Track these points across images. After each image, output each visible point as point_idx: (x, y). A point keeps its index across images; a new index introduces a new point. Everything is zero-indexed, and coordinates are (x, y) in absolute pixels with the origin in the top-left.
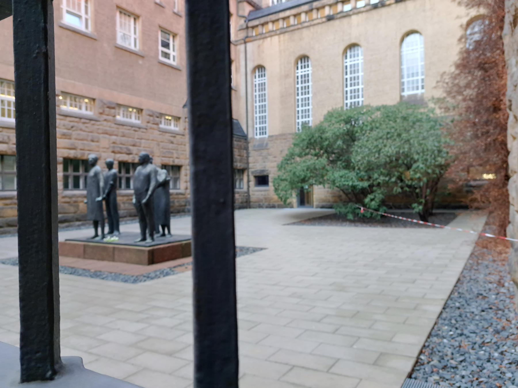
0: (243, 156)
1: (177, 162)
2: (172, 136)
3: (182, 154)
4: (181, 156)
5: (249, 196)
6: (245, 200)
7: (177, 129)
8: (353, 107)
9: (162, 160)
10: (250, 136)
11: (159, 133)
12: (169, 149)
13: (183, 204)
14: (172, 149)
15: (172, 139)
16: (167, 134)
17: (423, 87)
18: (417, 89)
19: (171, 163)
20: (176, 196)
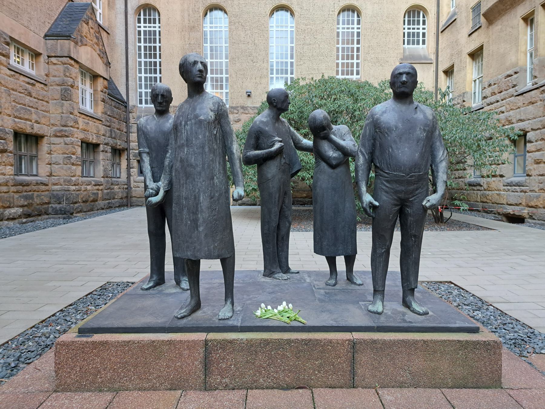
0: (123, 131)
1: (37, 129)
2: (28, 83)
3: (45, 117)
4: (43, 121)
5: (129, 188)
6: (125, 195)
7: (33, 73)
8: (289, 83)
9: (15, 121)
10: (131, 103)
11: (9, 72)
12: (25, 105)
13: (46, 200)
14: (29, 106)
15: (29, 87)
16: (22, 78)
17: (358, 73)
18: (352, 74)
19: (29, 130)
20: (35, 188)
